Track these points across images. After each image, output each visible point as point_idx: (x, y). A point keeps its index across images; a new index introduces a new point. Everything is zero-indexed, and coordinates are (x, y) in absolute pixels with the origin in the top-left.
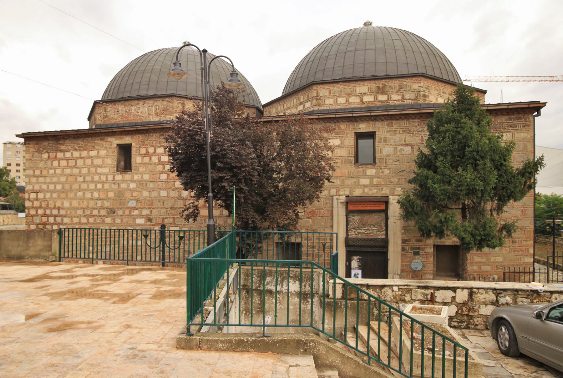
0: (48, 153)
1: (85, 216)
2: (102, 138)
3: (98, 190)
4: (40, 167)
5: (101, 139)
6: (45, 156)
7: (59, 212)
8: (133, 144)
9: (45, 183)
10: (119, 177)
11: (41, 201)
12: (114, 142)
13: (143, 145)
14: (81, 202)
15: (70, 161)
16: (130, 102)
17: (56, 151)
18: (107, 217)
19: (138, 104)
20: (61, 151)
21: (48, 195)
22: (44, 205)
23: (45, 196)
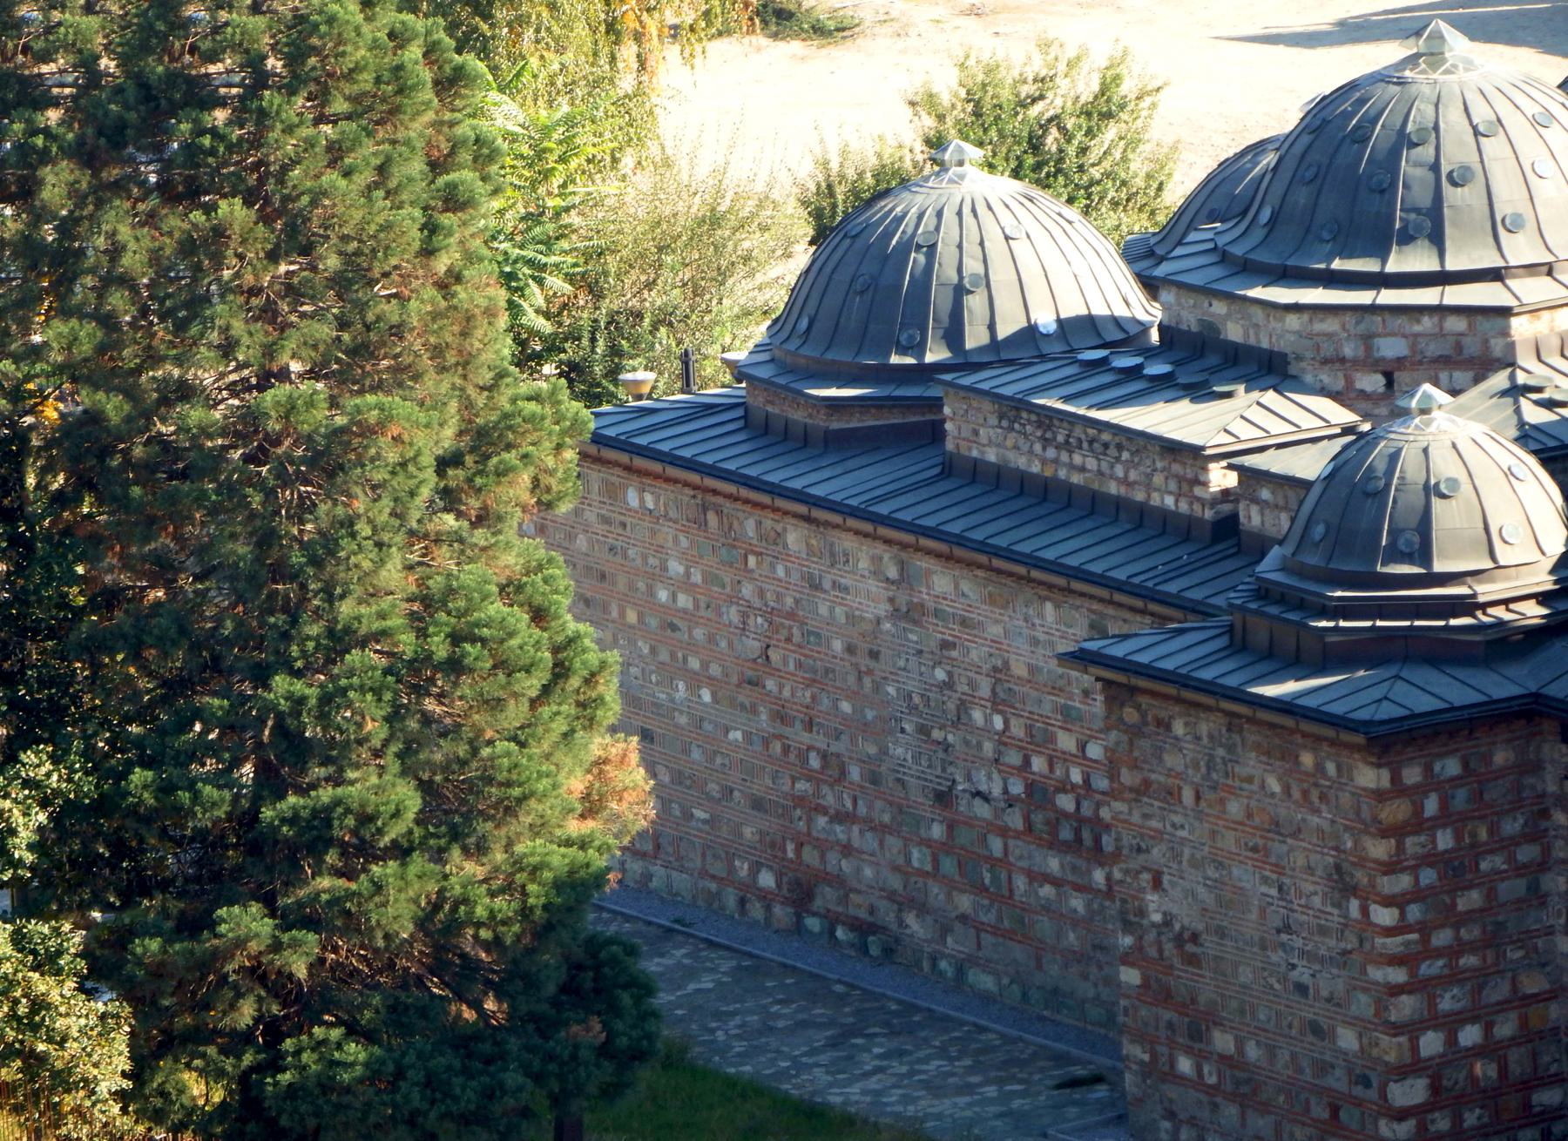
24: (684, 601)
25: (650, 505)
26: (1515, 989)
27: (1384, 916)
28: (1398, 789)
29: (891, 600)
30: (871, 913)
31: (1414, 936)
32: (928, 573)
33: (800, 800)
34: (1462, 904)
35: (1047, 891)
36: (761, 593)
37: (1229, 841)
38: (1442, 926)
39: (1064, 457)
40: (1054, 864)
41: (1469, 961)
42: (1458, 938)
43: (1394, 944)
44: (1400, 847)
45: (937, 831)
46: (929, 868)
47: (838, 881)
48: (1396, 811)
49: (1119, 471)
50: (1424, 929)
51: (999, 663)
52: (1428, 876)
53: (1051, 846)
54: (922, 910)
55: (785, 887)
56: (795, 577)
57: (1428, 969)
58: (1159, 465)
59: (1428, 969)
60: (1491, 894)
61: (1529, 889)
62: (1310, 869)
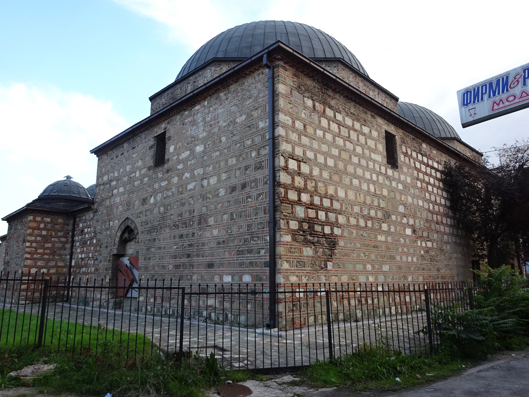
0: (312, 100)
1: (363, 216)
2: (373, 114)
3: (374, 183)
4: (303, 118)
5: (371, 115)
6: (309, 103)
7: (332, 203)
8: (397, 137)
9: (311, 149)
10: (390, 172)
11: (307, 178)
12: (384, 126)
13: (404, 143)
14: (358, 195)
15: (341, 127)
16: (369, 84)
17: (325, 103)
18: (383, 222)
19: (374, 91)
20: (331, 107)
21: (316, 172)
22: (310, 186)
23: (311, 172)
26: (56, 264)
27: (28, 244)
28: (34, 221)
31: (34, 249)
34: (46, 245)
37: (14, 243)
38: (41, 249)
41: (47, 257)
42: (44, 252)
43: (28, 250)
44: (33, 232)
48: (34, 225)
50: (36, 249)
52: (39, 238)
57: (35, 256)
59: (35, 256)
60: (54, 245)
61: (62, 246)
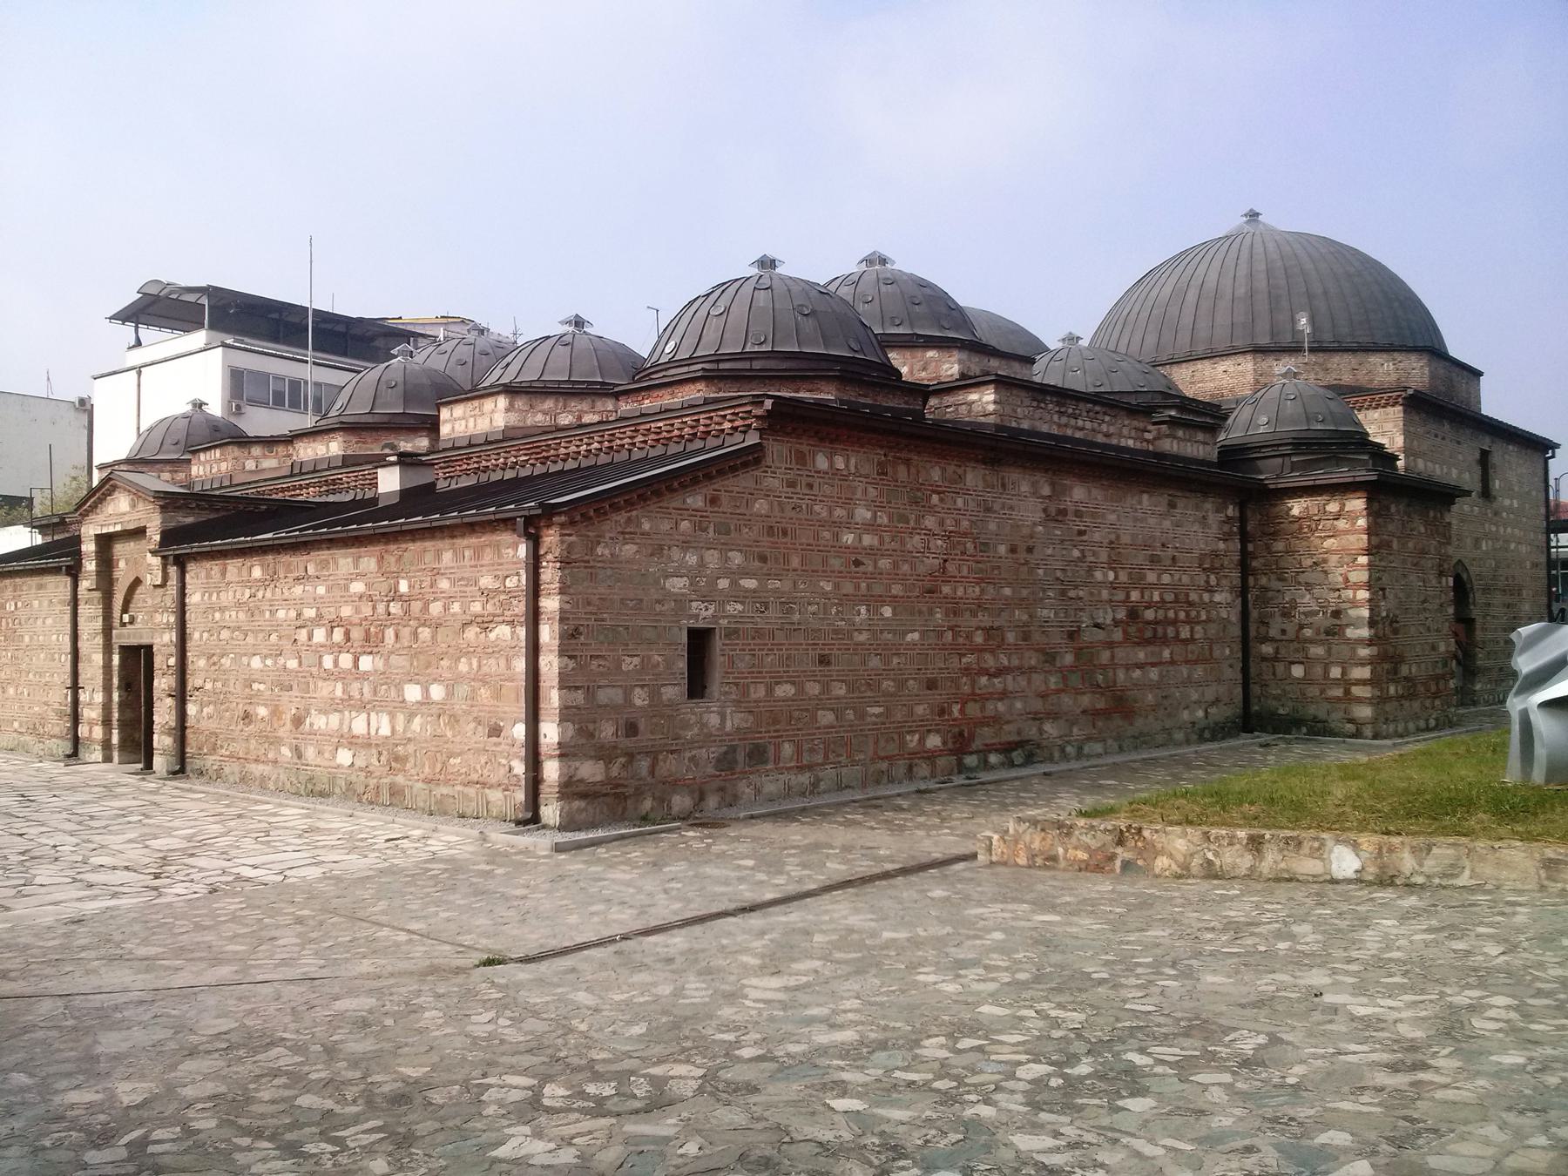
24: (868, 540)
25: (841, 466)
29: (1045, 510)
30: (1019, 733)
32: (1071, 488)
33: (966, 670)
35: (1137, 673)
36: (942, 523)
39: (1073, 422)
40: (1141, 655)
45: (1069, 659)
46: (1061, 686)
47: (996, 720)
49: (1104, 428)
51: (1113, 537)
53: (1138, 644)
54: (1054, 716)
55: (950, 741)
56: (972, 505)
58: (1126, 422)
62: (1432, 568)
